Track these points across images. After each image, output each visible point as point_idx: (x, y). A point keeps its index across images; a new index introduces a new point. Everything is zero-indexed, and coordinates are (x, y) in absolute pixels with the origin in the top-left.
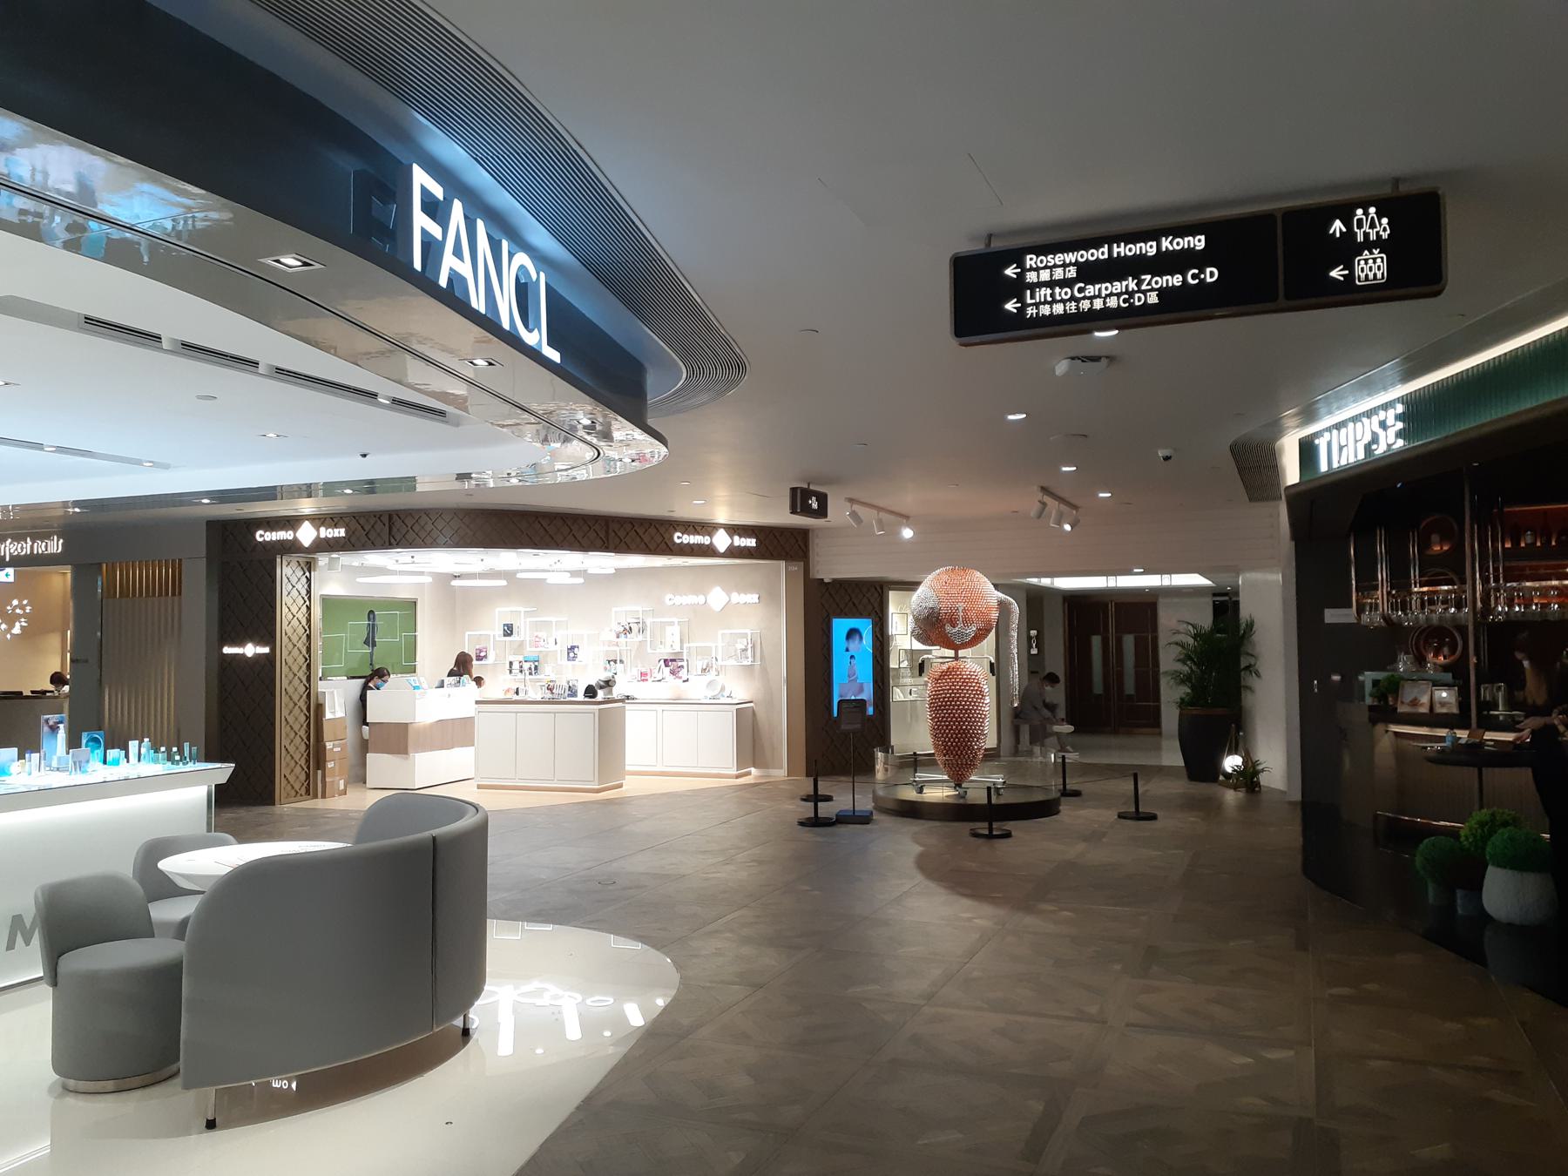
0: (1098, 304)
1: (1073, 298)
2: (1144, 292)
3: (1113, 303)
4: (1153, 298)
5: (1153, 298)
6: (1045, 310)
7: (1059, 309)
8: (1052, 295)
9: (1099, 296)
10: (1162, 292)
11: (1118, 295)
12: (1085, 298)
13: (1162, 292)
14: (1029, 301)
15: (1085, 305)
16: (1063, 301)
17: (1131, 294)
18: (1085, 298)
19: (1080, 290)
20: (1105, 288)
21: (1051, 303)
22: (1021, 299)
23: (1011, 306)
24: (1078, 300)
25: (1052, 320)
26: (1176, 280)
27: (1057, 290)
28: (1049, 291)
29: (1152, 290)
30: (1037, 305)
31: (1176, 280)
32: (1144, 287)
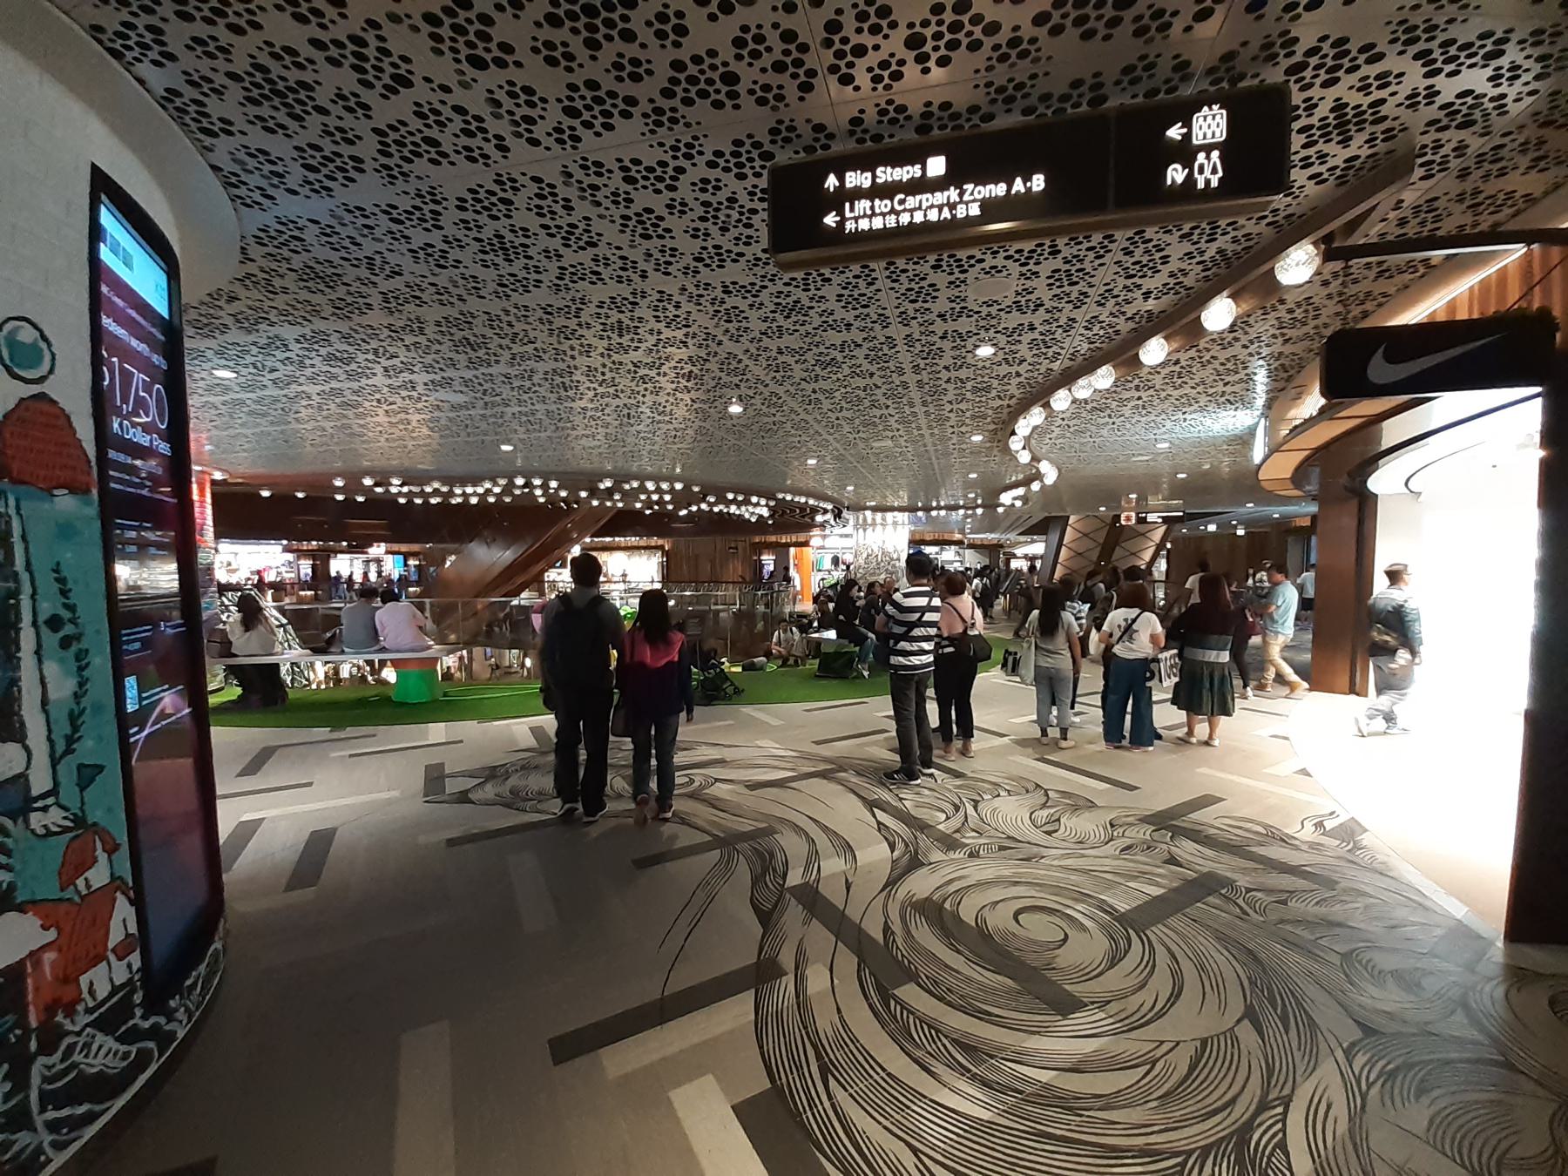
0: (918, 218)
1: (893, 211)
2: (967, 203)
3: (933, 216)
4: (975, 210)
5: (975, 210)
6: (864, 225)
7: (878, 223)
8: (872, 208)
9: (920, 208)
10: (985, 204)
11: (940, 208)
12: (905, 210)
13: (985, 204)
14: (848, 214)
15: (905, 219)
16: (883, 215)
17: (952, 207)
18: (905, 210)
19: (902, 202)
20: (926, 199)
21: (870, 217)
22: (841, 213)
23: (830, 220)
24: (897, 213)
25: (871, 235)
26: (1000, 190)
27: (877, 202)
28: (868, 204)
29: (974, 201)
30: (856, 219)
31: (1000, 190)
32: (966, 197)
